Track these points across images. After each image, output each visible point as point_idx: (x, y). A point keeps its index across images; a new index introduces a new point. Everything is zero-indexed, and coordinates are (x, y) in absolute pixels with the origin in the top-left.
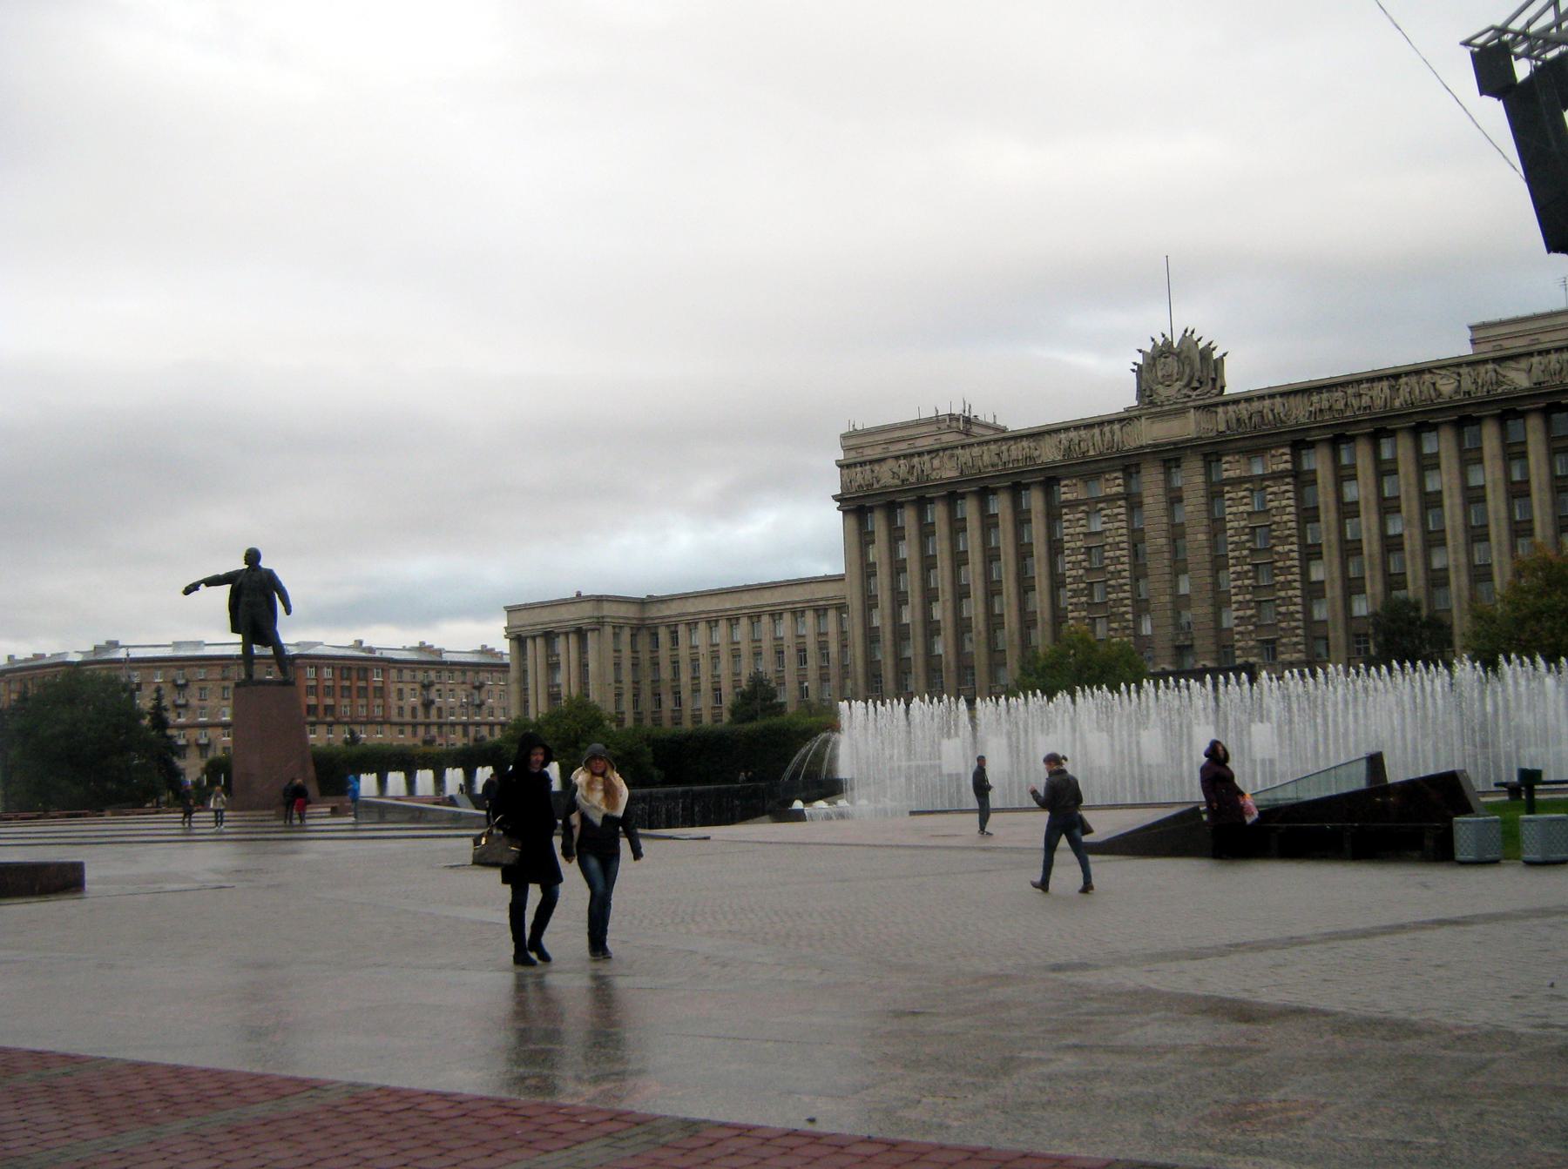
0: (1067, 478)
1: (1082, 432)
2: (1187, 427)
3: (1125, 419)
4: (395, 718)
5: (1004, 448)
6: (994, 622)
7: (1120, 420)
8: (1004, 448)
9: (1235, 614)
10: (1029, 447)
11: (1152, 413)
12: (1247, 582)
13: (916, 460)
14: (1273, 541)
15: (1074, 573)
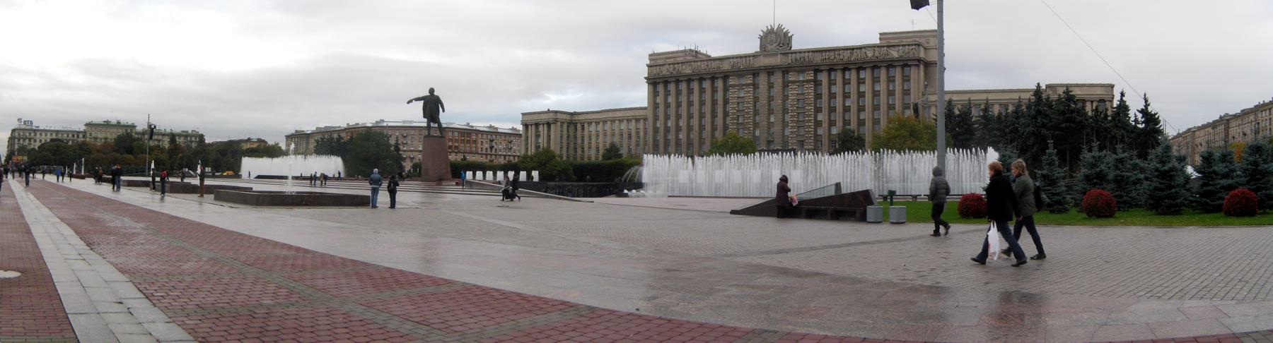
0: (732, 76)
1: (739, 59)
2: (777, 60)
3: (755, 56)
4: (480, 152)
5: (710, 63)
6: (702, 128)
7: (753, 56)
8: (710, 63)
9: (790, 130)
13: (676, 65)
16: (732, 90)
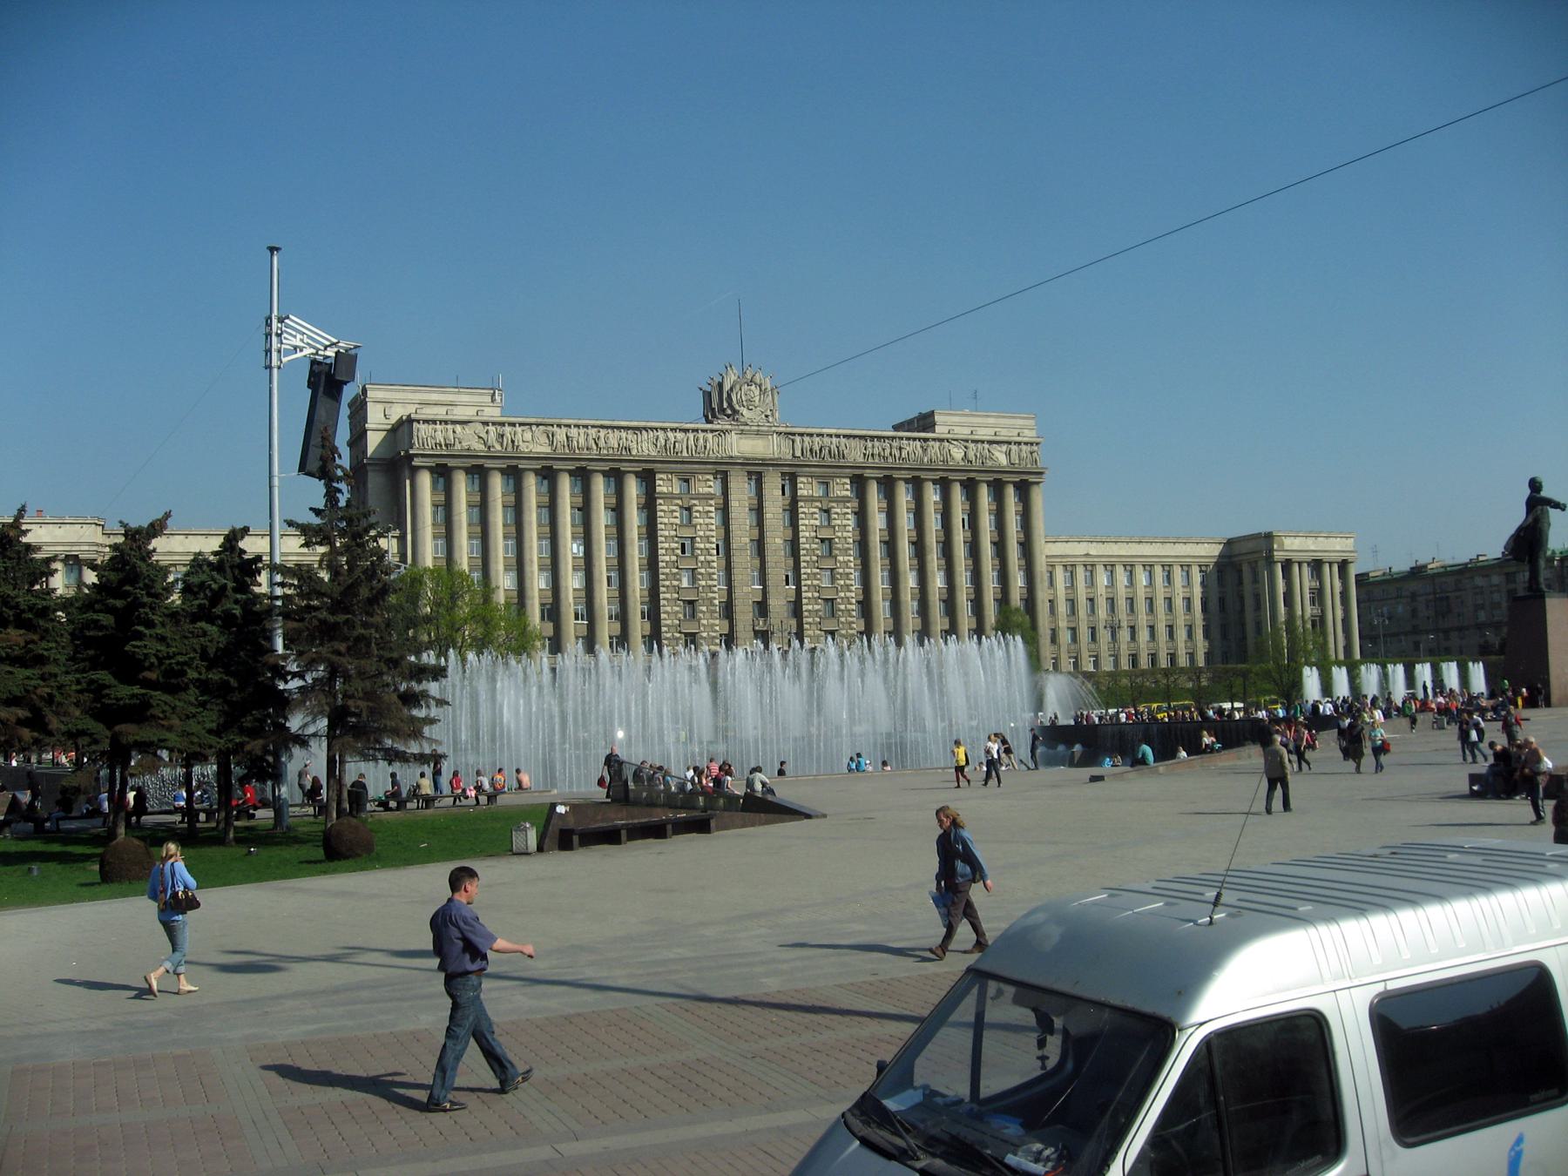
0: (659, 472)
1: (680, 435)
12: (815, 582)
14: (837, 552)
15: (667, 558)
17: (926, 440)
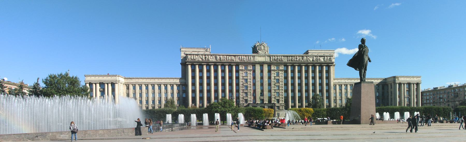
0: (240, 65)
1: (244, 57)
10: (233, 58)
11: (258, 56)
14: (280, 82)
16: (240, 72)
17: (307, 56)
